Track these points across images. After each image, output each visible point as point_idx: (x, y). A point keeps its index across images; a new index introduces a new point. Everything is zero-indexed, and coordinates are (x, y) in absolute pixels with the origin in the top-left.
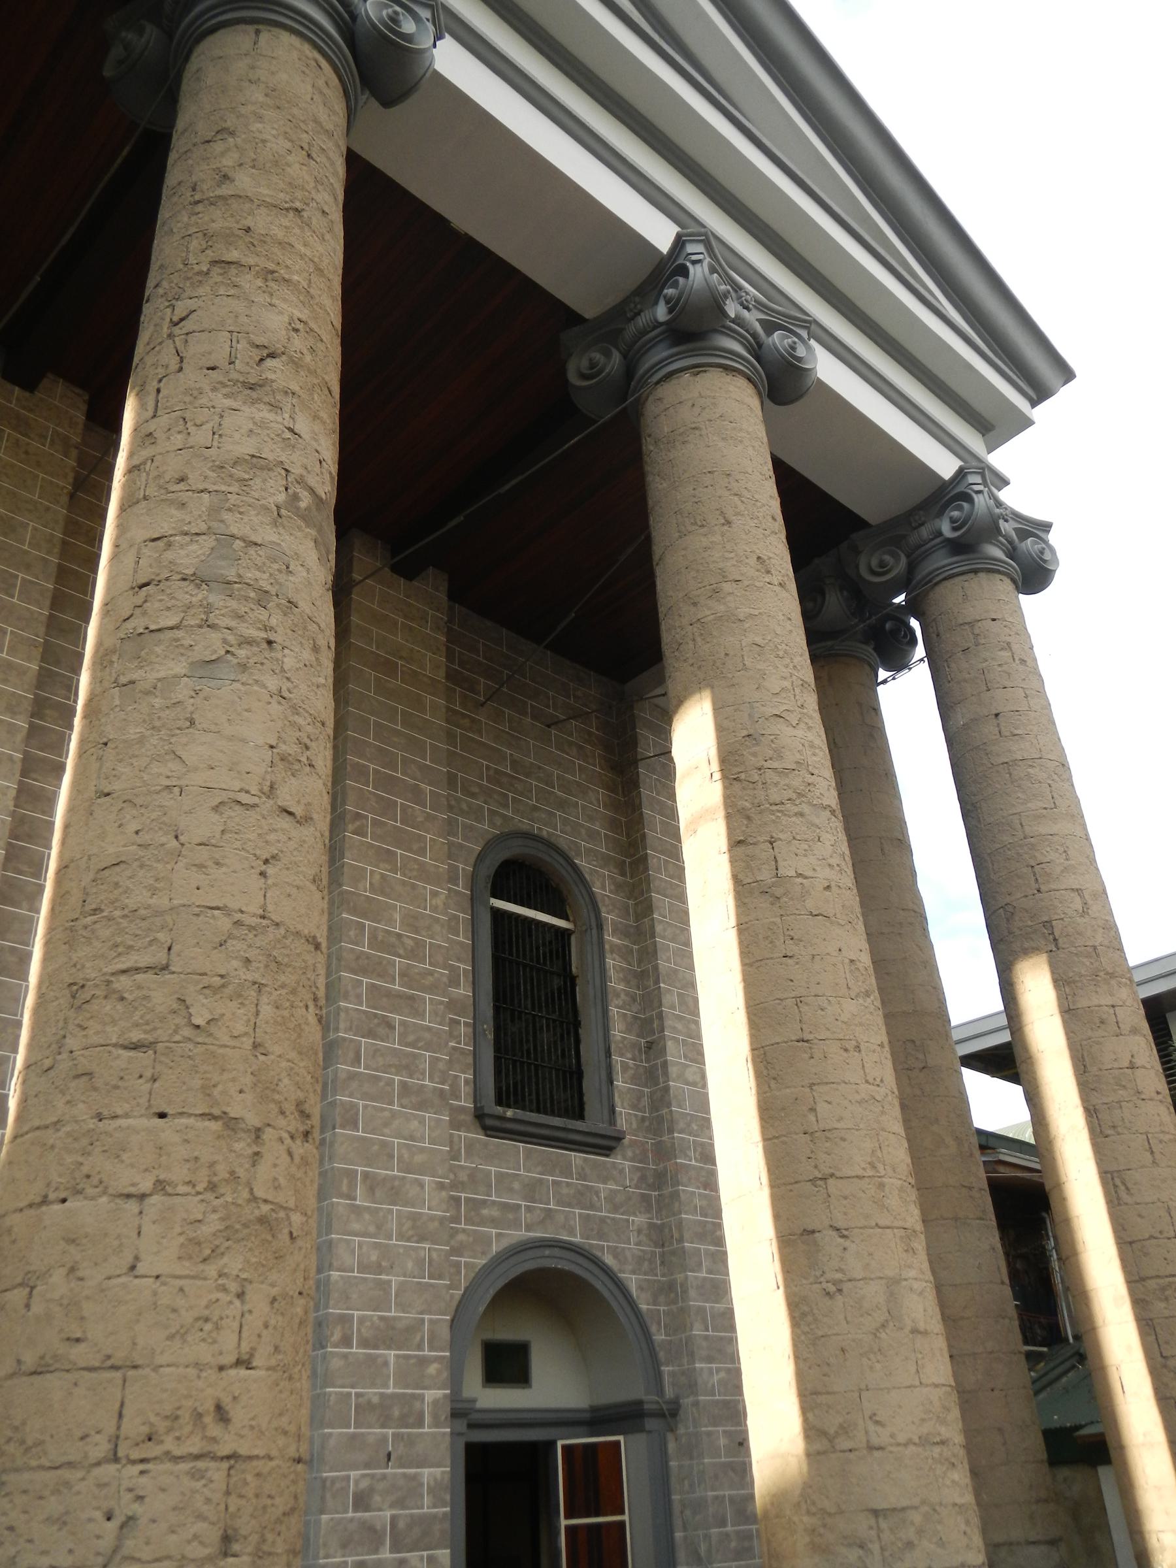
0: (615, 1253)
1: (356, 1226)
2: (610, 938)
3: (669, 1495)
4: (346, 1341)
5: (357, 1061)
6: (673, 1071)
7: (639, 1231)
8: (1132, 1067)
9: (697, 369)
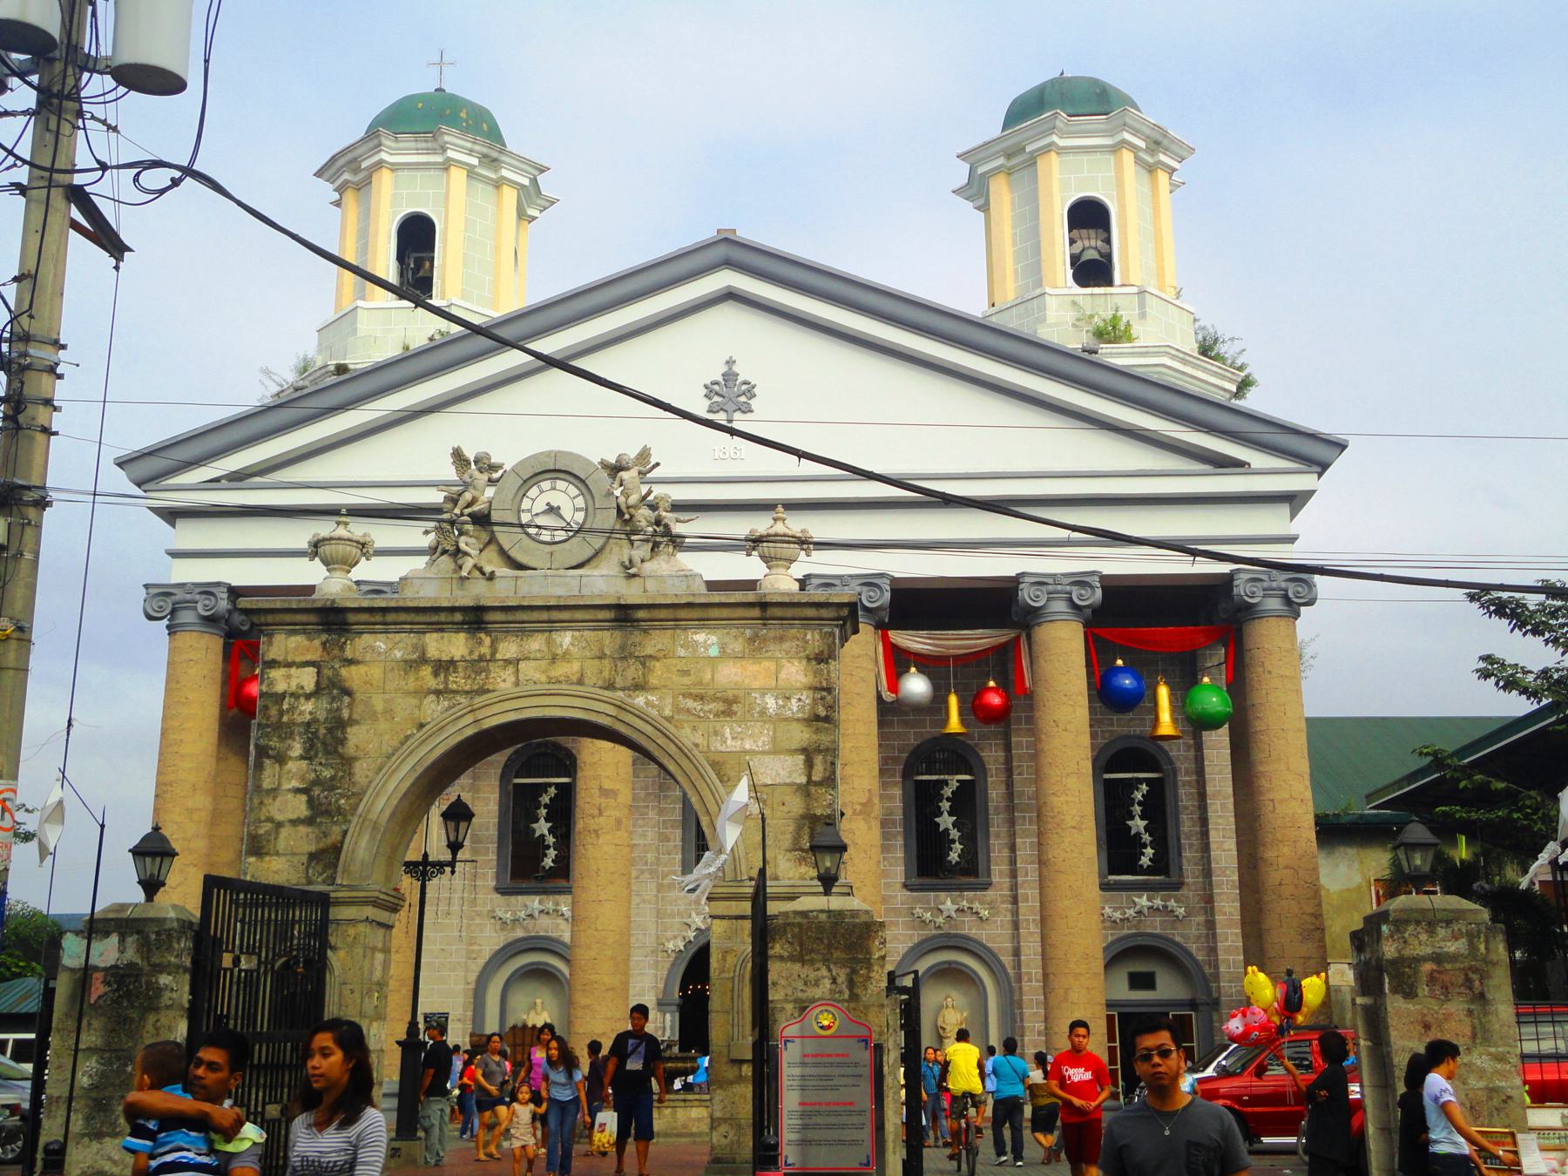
0: (1182, 936)
1: (1031, 939)
2: (1182, 778)
3: (1213, 1036)
4: (1030, 981)
5: (1027, 875)
6: (1213, 846)
7: (1198, 925)
8: (1280, 884)
9: (1039, 624)
